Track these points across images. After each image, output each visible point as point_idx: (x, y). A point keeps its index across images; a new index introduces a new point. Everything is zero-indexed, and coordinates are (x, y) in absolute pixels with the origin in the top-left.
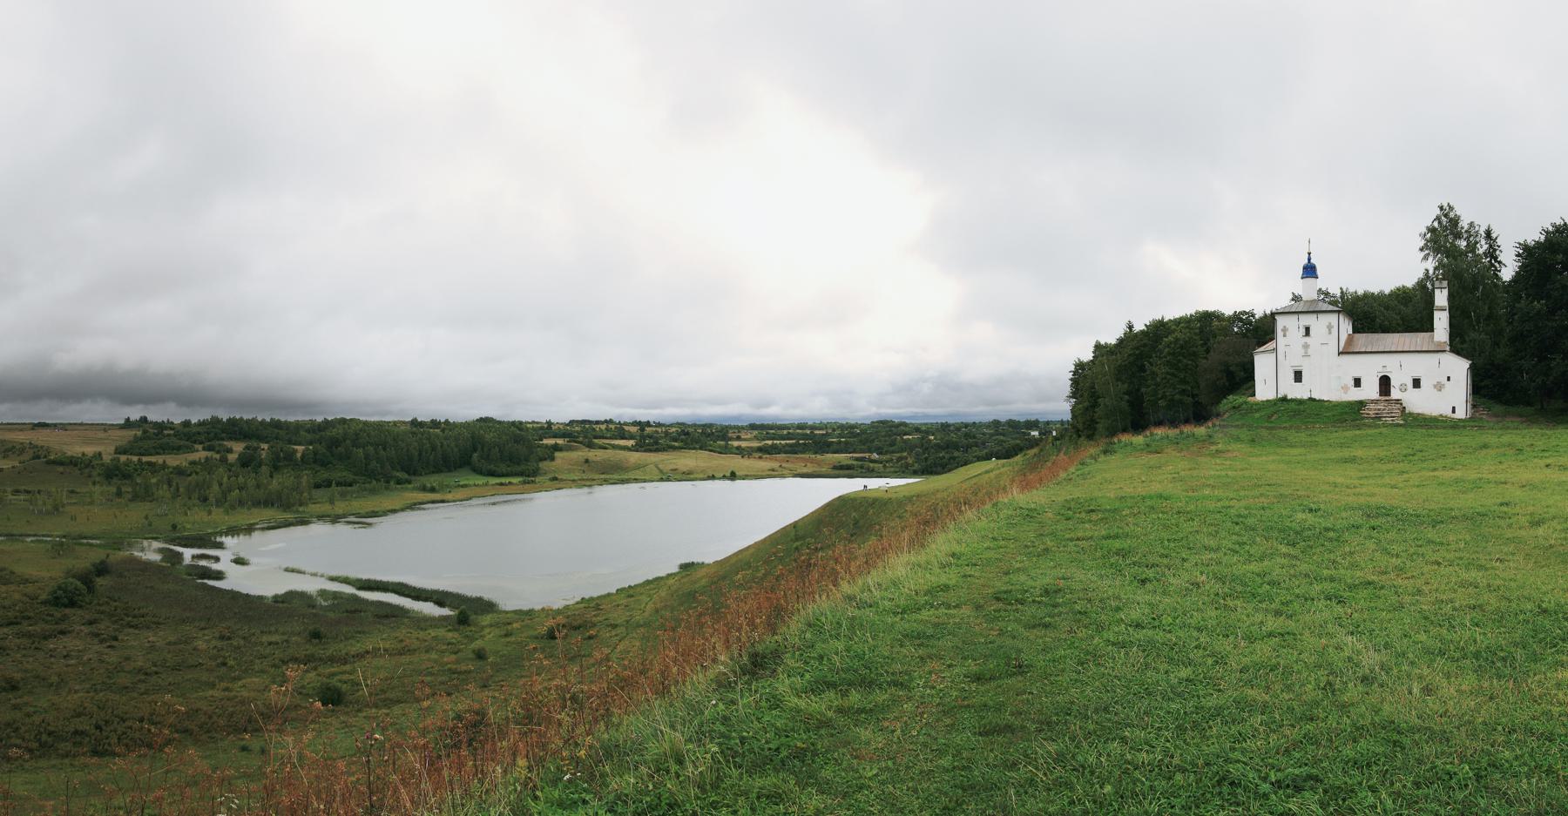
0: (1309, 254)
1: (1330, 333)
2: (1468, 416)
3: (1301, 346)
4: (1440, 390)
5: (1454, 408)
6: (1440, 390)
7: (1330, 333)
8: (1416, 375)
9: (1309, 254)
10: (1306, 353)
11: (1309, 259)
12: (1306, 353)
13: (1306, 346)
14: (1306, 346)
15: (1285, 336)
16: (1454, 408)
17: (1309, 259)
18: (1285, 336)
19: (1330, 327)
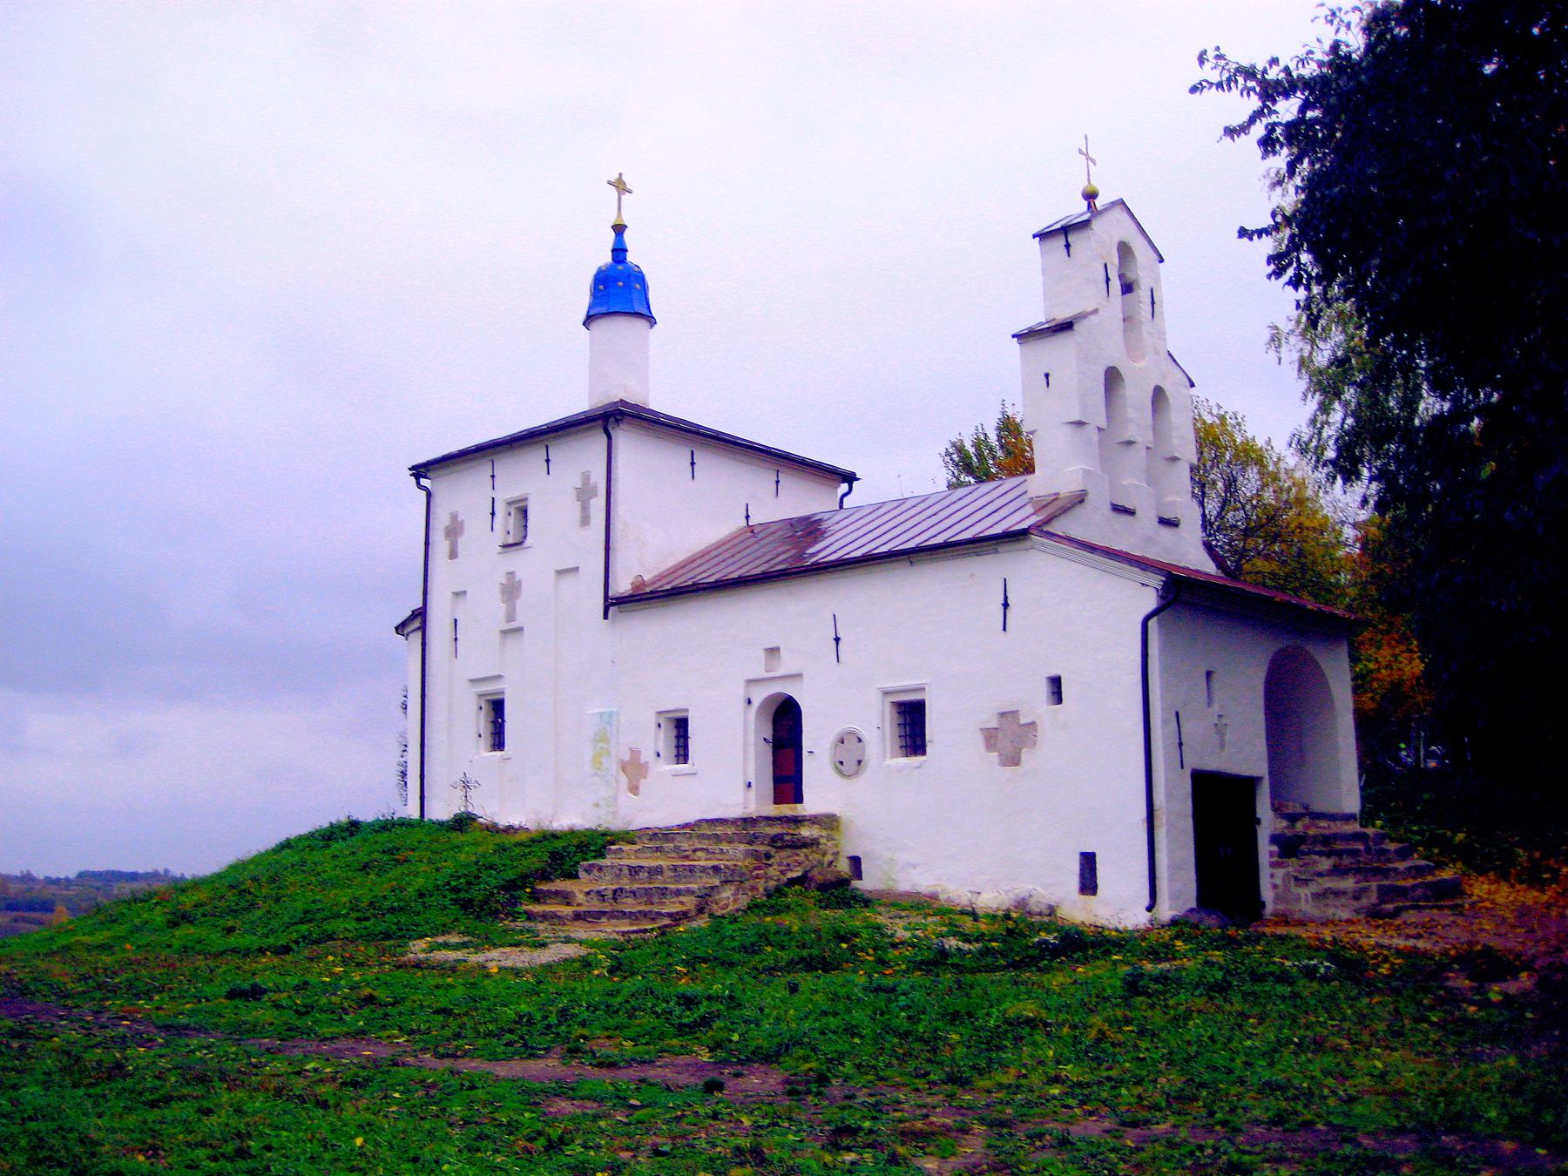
0: (619, 229)
1: (585, 520)
2: (1165, 912)
3: (497, 591)
4: (1015, 761)
5: (1088, 862)
6: (1015, 761)
7: (585, 520)
8: (904, 680)
9: (619, 229)
10: (511, 617)
11: (619, 252)
12: (511, 617)
13: (511, 590)
14: (511, 590)
15: (453, 554)
16: (1088, 862)
17: (619, 252)
18: (453, 554)
19: (584, 495)
